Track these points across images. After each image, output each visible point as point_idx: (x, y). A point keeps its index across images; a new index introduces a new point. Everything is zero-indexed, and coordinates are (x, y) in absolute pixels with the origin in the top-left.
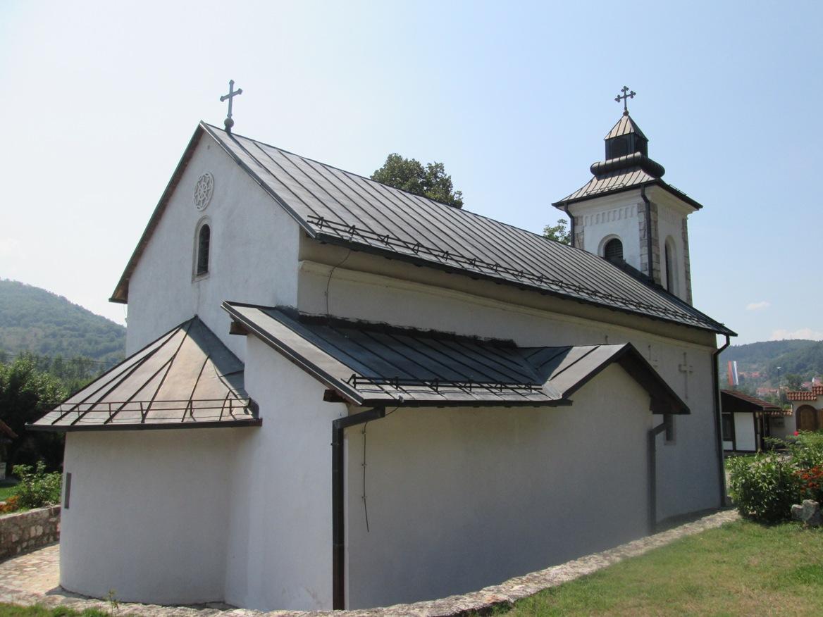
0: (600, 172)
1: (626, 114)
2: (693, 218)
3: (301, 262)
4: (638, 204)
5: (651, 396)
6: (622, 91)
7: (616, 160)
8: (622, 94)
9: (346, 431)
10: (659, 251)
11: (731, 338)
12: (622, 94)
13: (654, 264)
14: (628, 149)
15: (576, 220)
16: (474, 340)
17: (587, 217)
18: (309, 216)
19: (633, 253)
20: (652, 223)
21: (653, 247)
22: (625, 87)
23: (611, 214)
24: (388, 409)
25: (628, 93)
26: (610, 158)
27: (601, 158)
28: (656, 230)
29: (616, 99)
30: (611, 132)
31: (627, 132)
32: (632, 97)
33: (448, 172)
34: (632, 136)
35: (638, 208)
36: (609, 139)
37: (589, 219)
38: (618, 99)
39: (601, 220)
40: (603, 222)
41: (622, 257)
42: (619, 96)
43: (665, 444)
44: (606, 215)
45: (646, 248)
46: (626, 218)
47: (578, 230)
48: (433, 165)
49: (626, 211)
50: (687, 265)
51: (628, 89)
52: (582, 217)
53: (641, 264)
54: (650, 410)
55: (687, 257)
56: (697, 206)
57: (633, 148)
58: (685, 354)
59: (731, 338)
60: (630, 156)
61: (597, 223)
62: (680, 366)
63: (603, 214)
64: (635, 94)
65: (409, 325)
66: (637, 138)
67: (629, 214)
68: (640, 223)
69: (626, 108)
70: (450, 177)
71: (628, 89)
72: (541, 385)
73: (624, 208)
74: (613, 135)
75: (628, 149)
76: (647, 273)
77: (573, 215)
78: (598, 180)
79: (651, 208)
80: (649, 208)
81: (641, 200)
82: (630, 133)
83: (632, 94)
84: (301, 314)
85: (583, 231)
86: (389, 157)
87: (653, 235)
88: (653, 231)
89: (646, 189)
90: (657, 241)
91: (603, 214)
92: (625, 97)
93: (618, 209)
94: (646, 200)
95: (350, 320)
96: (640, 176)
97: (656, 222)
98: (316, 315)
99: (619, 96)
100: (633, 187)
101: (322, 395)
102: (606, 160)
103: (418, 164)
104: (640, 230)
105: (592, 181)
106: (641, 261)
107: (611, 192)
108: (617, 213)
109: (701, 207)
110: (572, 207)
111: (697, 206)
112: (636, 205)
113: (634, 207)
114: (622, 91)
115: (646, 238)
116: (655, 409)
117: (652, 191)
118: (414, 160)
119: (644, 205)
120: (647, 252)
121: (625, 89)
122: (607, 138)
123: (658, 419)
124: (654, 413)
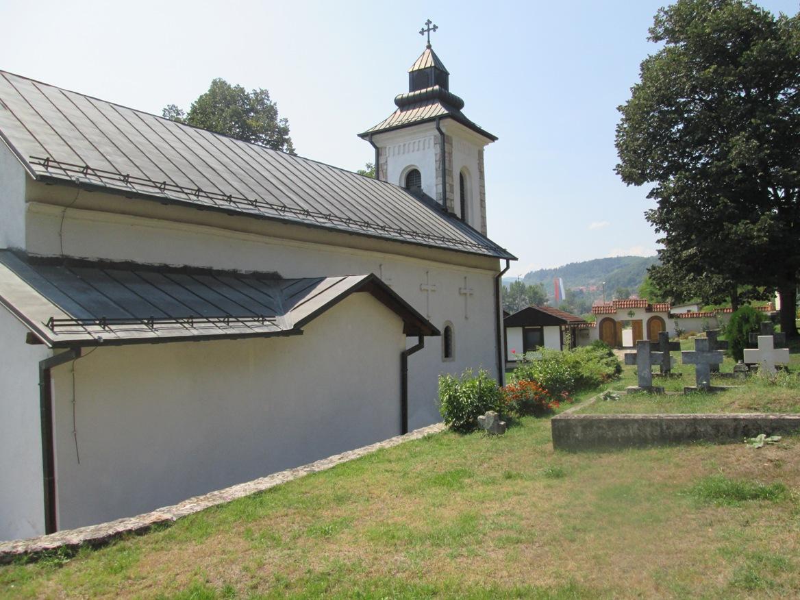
0: (403, 104)
1: (429, 47)
2: (489, 150)
3: (28, 204)
5: (404, 321)
6: (426, 24)
7: (417, 92)
8: (426, 28)
9: (53, 371)
10: (453, 181)
11: (511, 262)
12: (426, 28)
13: (447, 193)
14: (430, 82)
15: (380, 150)
16: (234, 274)
18: (30, 157)
19: (430, 184)
20: (446, 155)
21: (447, 177)
22: (429, 20)
23: (411, 146)
24: (84, 350)
25: (431, 26)
27: (405, 91)
28: (450, 161)
29: (420, 32)
31: (428, 65)
32: (435, 31)
33: (274, 98)
34: (433, 69)
35: (435, 139)
36: (413, 72)
37: (392, 149)
38: (422, 32)
41: (421, 186)
42: (423, 29)
43: (443, 361)
44: (407, 145)
46: (424, 149)
47: (382, 161)
48: (258, 91)
50: (482, 194)
51: (431, 22)
53: (437, 193)
54: (404, 333)
55: (482, 186)
56: (493, 138)
58: (465, 278)
59: (511, 262)
60: (430, 89)
61: (399, 154)
62: (460, 289)
63: (405, 145)
64: (437, 27)
65: (158, 262)
66: (437, 71)
67: (427, 145)
68: (436, 154)
69: (429, 42)
70: (275, 104)
71: (431, 22)
72: (274, 317)
74: (416, 68)
75: (430, 82)
76: (441, 202)
77: (378, 146)
78: (402, 111)
79: (446, 140)
80: (444, 140)
81: (437, 133)
82: (431, 66)
83: (435, 28)
84: (30, 255)
85: (386, 162)
86: (213, 82)
90: (451, 172)
91: (405, 145)
92: (429, 30)
94: (441, 133)
95: (89, 260)
96: (437, 109)
97: (450, 154)
98: (49, 256)
99: (423, 29)
100: (430, 120)
101: (25, 338)
102: (410, 92)
103: (242, 90)
104: (436, 161)
105: (395, 112)
106: (437, 190)
107: (410, 125)
109: (497, 139)
110: (375, 138)
111: (493, 138)
112: (433, 137)
113: (431, 139)
114: (426, 24)
115: (441, 168)
116: (409, 332)
117: (446, 124)
118: (238, 85)
119: (440, 138)
120: (441, 182)
121: (429, 22)
122: (411, 70)
123: (414, 341)
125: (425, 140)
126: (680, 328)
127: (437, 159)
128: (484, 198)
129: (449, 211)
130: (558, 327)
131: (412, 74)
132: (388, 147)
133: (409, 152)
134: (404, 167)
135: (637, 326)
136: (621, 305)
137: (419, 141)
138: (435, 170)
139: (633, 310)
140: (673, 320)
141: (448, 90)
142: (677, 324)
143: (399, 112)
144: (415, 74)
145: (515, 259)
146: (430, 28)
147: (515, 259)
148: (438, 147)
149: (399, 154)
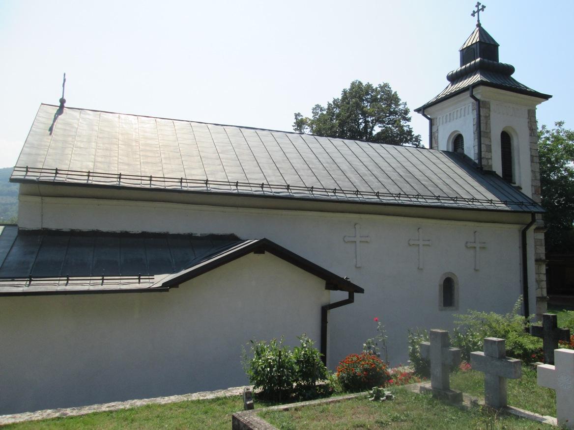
1: (479, 25)
7: (468, 65)
8: (476, 9)
10: (490, 141)
12: (476, 9)
13: (483, 153)
15: (433, 121)
16: (190, 237)
20: (482, 118)
21: (482, 138)
25: (480, 7)
26: (463, 65)
34: (478, 44)
35: (473, 106)
36: (463, 50)
37: (441, 120)
38: (473, 15)
42: (474, 11)
44: (452, 115)
47: (434, 130)
49: (453, 114)
51: (480, 4)
52: (437, 118)
56: (546, 97)
61: (446, 122)
63: (450, 114)
65: (120, 230)
69: (478, 21)
70: (396, 92)
72: (153, 276)
74: (465, 46)
76: (477, 161)
80: (480, 105)
81: (473, 100)
82: (476, 42)
83: (484, 7)
85: (438, 130)
91: (450, 114)
92: (478, 11)
93: (459, 109)
95: (63, 230)
97: (488, 117)
98: (34, 229)
99: (474, 11)
102: (461, 66)
104: (474, 125)
106: (474, 152)
109: (551, 96)
111: (546, 97)
112: (471, 104)
117: (480, 91)
118: (368, 83)
121: (479, 4)
125: (465, 108)
127: (475, 123)
129: (485, 169)
131: (462, 51)
132: (438, 117)
133: (453, 119)
134: (451, 132)
138: (473, 134)
141: (497, 60)
146: (480, 8)
149: (446, 122)
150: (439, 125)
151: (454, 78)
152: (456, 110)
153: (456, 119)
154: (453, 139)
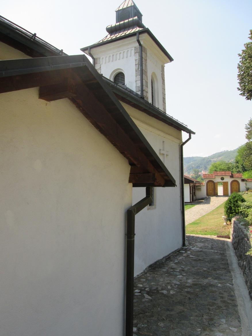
2: (168, 67)
4: (135, 48)
5: (131, 164)
11: (192, 135)
13: (144, 87)
15: (96, 60)
17: (103, 58)
20: (143, 60)
23: (118, 56)
27: (113, 22)
30: (120, 7)
31: (129, 5)
36: (119, 11)
39: (111, 59)
40: (112, 61)
44: (115, 56)
45: (140, 76)
46: (127, 57)
50: (164, 94)
52: (100, 58)
54: (130, 182)
55: (164, 89)
57: (133, 16)
59: (192, 135)
60: (131, 19)
61: (109, 61)
62: (160, 150)
63: (113, 55)
67: (129, 55)
73: (126, 51)
74: (121, 8)
76: (139, 93)
77: (95, 57)
79: (143, 50)
80: (142, 49)
81: (137, 44)
85: (100, 68)
87: (144, 68)
88: (144, 65)
89: (140, 36)
90: (146, 72)
91: (113, 55)
93: (122, 52)
94: (140, 44)
97: (146, 60)
100: (134, 34)
102: (117, 22)
104: (136, 65)
105: (107, 36)
108: (122, 55)
110: (93, 51)
111: (171, 59)
112: (133, 49)
115: (139, 69)
116: (136, 180)
119: (139, 49)
122: (117, 10)
123: (141, 193)
124: (135, 185)
125: (128, 51)
126: (248, 186)
127: (137, 63)
128: (165, 97)
130: (189, 184)
133: (116, 60)
135: (225, 185)
136: (218, 174)
137: (124, 52)
138: (135, 72)
139: (224, 177)
140: (244, 182)
142: (246, 184)
143: (109, 36)
144: (120, 12)
145: (194, 133)
147: (194, 133)
148: (137, 55)
149: (109, 61)
150: (102, 64)
151: (111, 31)
152: (123, 51)
153: (119, 59)
154: (115, 75)
